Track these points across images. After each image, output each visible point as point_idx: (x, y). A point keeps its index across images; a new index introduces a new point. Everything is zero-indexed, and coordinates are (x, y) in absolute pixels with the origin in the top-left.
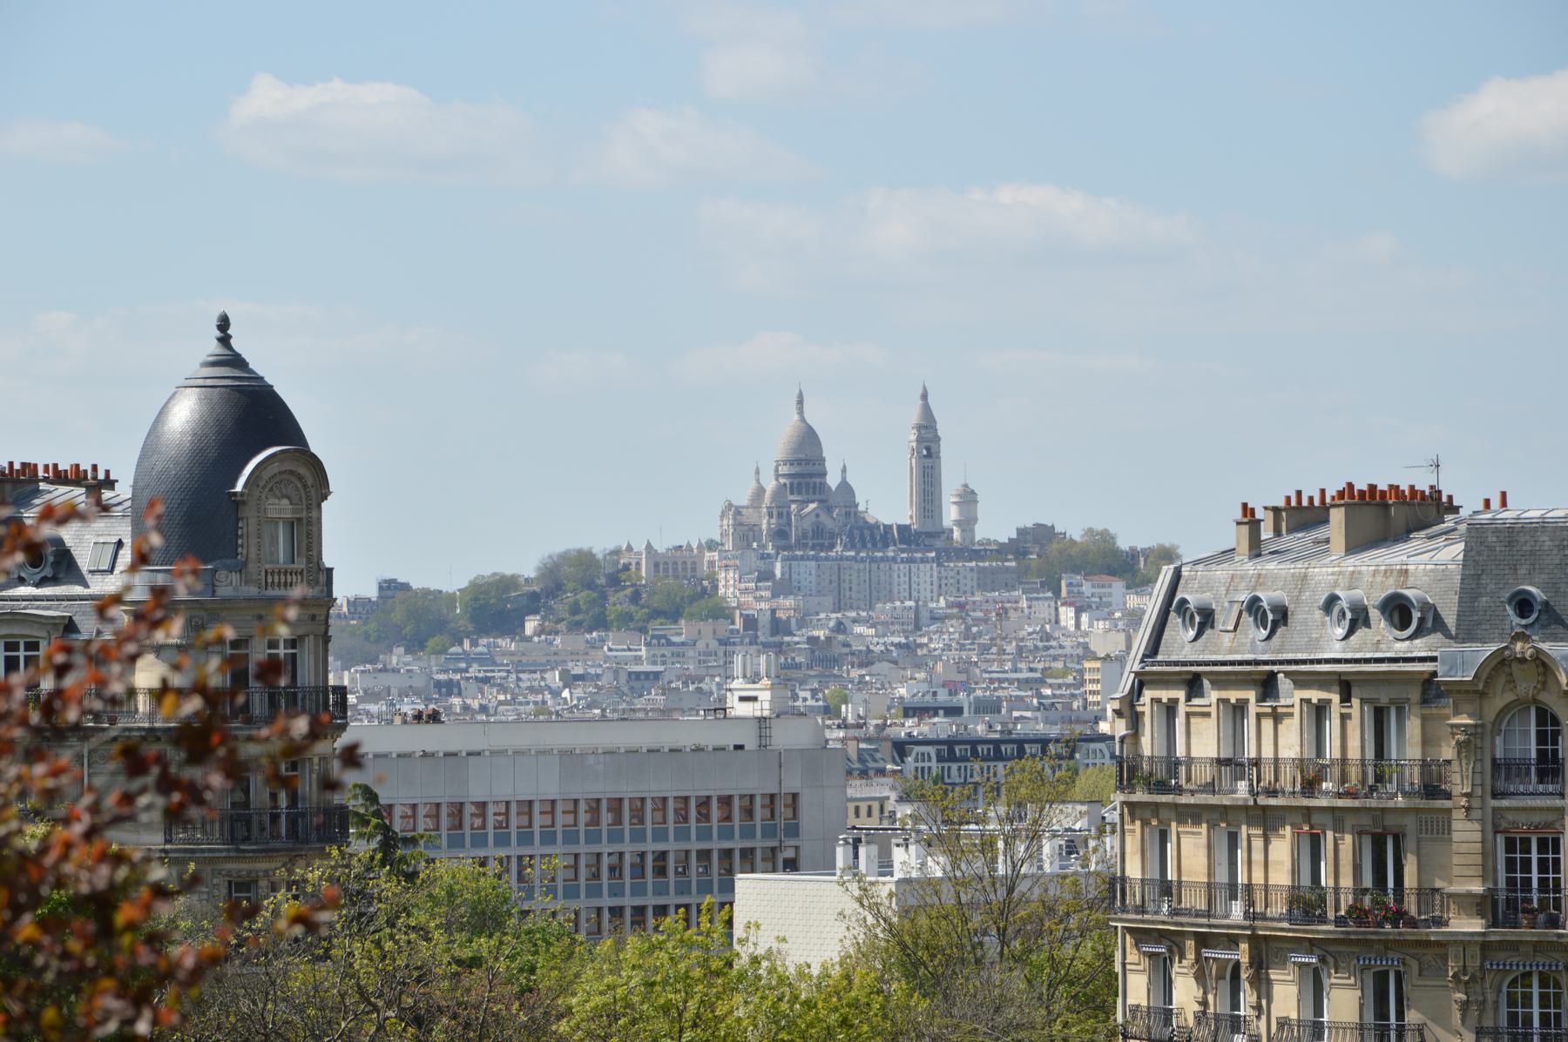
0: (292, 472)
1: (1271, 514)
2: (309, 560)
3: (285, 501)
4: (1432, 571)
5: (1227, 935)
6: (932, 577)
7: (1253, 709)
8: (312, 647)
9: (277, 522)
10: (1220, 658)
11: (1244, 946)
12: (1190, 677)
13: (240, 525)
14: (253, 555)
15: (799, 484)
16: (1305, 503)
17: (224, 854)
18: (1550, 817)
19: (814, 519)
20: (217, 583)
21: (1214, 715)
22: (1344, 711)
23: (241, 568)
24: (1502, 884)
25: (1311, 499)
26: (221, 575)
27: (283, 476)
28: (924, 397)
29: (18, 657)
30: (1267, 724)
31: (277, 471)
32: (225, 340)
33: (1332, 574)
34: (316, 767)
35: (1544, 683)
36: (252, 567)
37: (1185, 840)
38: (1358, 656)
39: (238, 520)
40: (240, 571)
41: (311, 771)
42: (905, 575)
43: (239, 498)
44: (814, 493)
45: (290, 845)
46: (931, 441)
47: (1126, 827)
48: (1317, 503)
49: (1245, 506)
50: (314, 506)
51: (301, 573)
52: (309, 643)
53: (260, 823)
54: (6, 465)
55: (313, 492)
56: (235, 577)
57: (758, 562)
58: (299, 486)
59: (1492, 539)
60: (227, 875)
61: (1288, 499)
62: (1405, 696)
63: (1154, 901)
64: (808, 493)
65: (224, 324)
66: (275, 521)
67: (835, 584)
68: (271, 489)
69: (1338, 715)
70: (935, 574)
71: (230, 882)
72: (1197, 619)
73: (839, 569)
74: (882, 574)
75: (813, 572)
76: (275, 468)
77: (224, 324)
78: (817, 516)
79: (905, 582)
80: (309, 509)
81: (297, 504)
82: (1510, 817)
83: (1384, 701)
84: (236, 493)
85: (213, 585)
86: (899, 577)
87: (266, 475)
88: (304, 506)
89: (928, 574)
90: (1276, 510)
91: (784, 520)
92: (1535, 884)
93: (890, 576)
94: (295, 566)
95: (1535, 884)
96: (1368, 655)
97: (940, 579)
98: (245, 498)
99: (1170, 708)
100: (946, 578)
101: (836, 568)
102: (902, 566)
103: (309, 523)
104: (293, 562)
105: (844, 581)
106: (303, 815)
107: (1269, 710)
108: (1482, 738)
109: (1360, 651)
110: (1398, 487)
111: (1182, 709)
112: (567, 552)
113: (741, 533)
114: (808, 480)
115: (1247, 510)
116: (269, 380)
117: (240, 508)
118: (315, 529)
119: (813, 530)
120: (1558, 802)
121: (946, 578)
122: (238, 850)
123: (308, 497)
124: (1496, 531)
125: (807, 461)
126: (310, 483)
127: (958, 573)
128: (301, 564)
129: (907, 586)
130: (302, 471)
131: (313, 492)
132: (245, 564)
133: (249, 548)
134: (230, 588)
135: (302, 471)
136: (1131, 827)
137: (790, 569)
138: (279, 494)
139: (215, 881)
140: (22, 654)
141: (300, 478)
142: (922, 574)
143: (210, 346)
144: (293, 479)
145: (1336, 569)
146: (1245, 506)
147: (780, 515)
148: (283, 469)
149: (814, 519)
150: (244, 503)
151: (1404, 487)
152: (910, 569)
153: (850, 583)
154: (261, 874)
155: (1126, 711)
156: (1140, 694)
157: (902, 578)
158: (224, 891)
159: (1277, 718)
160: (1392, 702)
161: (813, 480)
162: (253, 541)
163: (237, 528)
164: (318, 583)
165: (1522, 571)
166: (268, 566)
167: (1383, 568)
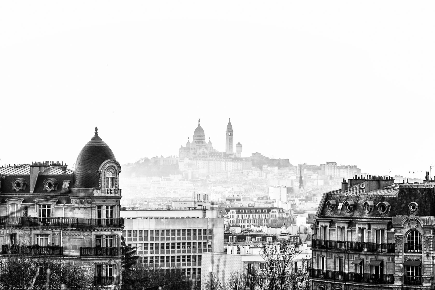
0: (112, 166)
1: (349, 181)
2: (116, 187)
3: (111, 173)
4: (390, 197)
5: (339, 284)
7: (346, 229)
8: (116, 208)
9: (108, 178)
10: (338, 216)
11: (343, 286)
12: (330, 221)
13: (100, 179)
14: (103, 186)
15: (199, 141)
16: (358, 178)
17: (95, 258)
18: (418, 258)
20: (94, 193)
21: (336, 230)
22: (369, 231)
23: (100, 189)
24: (406, 274)
25: (359, 177)
26: (95, 191)
27: (110, 167)
28: (230, 120)
29: (45, 209)
30: (350, 234)
31: (109, 166)
32: (96, 133)
33: (366, 197)
34: (117, 237)
35: (417, 225)
36: (103, 189)
37: (329, 260)
38: (372, 217)
39: (99, 177)
40: (100, 190)
41: (116, 238)
43: (100, 172)
45: (111, 257)
47: (314, 256)
48: (360, 178)
49: (344, 179)
50: (118, 174)
51: (114, 190)
52: (116, 207)
53: (103, 251)
54: (43, 163)
55: (117, 171)
56: (98, 191)
58: (114, 169)
59: (405, 190)
60: (95, 263)
61: (353, 177)
62: (384, 228)
63: (321, 275)
65: (96, 129)
66: (107, 178)
68: (107, 170)
69: (367, 232)
71: (96, 265)
72: (332, 207)
76: (108, 165)
77: (96, 129)
78: (203, 149)
80: (116, 175)
81: (113, 173)
82: (409, 257)
83: (379, 228)
84: (99, 171)
85: (93, 193)
87: (106, 167)
88: (115, 174)
90: (351, 180)
91: (195, 150)
92: (414, 274)
94: (113, 189)
95: (414, 274)
96: (375, 217)
97: (233, 165)
98: (101, 172)
99: (325, 228)
102: (224, 162)
103: (116, 178)
104: (112, 188)
106: (114, 249)
107: (350, 230)
108: (402, 238)
109: (372, 216)
110: (381, 176)
111: (328, 229)
115: (344, 181)
116: (107, 144)
117: (100, 174)
118: (117, 180)
120: (420, 255)
122: (98, 257)
123: (116, 172)
124: (406, 189)
125: (201, 136)
126: (117, 168)
127: (237, 164)
128: (114, 188)
129: (225, 167)
130: (115, 166)
131: (117, 170)
132: (101, 188)
133: (102, 184)
134: (97, 194)
135: (115, 166)
136: (315, 256)
138: (109, 171)
139: (93, 265)
140: (46, 208)
141: (114, 167)
143: (93, 135)
144: (113, 167)
145: (367, 196)
146: (344, 179)
147: (194, 149)
148: (110, 165)
150: (101, 173)
151: (383, 176)
154: (103, 263)
155: (314, 228)
156: (318, 224)
158: (94, 267)
159: (351, 231)
160: (380, 229)
162: (103, 182)
163: (99, 179)
164: (118, 193)
165: (413, 198)
166: (106, 189)
167: (378, 196)
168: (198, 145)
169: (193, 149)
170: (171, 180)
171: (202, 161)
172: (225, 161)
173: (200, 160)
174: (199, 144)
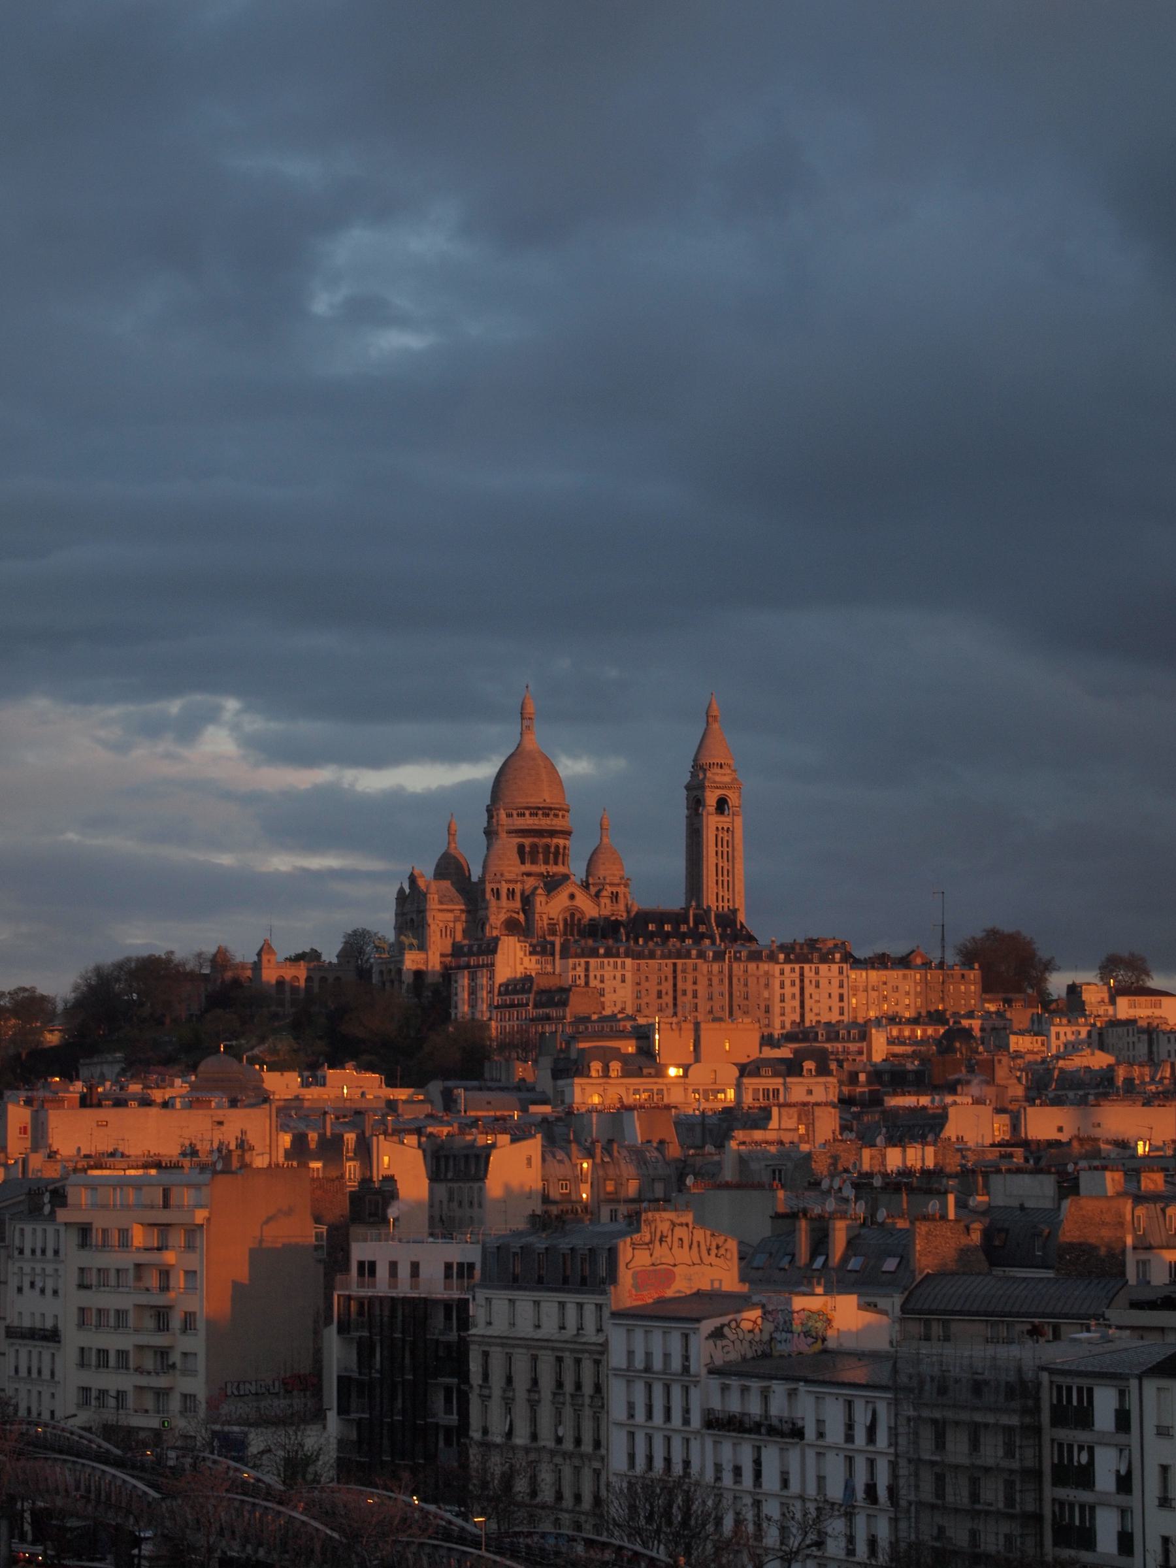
15: (534, 847)
19: (567, 903)
42: (793, 984)
44: (556, 863)
46: (730, 788)
57: (526, 959)
64: (546, 862)
67: (668, 999)
73: (675, 971)
74: (752, 981)
75: (629, 975)
79: (794, 996)
86: (782, 987)
89: (836, 983)
93: (767, 986)
101: (669, 971)
102: (787, 968)
105: (684, 993)
112: (129, 960)
113: (441, 924)
114: (548, 840)
119: (565, 920)
125: (547, 811)
129: (797, 1003)
137: (587, 970)
142: (823, 982)
149: (567, 903)
152: (802, 975)
153: (695, 996)
157: (788, 990)
161: (555, 841)
168: (528, 867)
169: (504, 892)
171: (628, 961)
172: (797, 961)
173: (608, 954)
174: (534, 862)
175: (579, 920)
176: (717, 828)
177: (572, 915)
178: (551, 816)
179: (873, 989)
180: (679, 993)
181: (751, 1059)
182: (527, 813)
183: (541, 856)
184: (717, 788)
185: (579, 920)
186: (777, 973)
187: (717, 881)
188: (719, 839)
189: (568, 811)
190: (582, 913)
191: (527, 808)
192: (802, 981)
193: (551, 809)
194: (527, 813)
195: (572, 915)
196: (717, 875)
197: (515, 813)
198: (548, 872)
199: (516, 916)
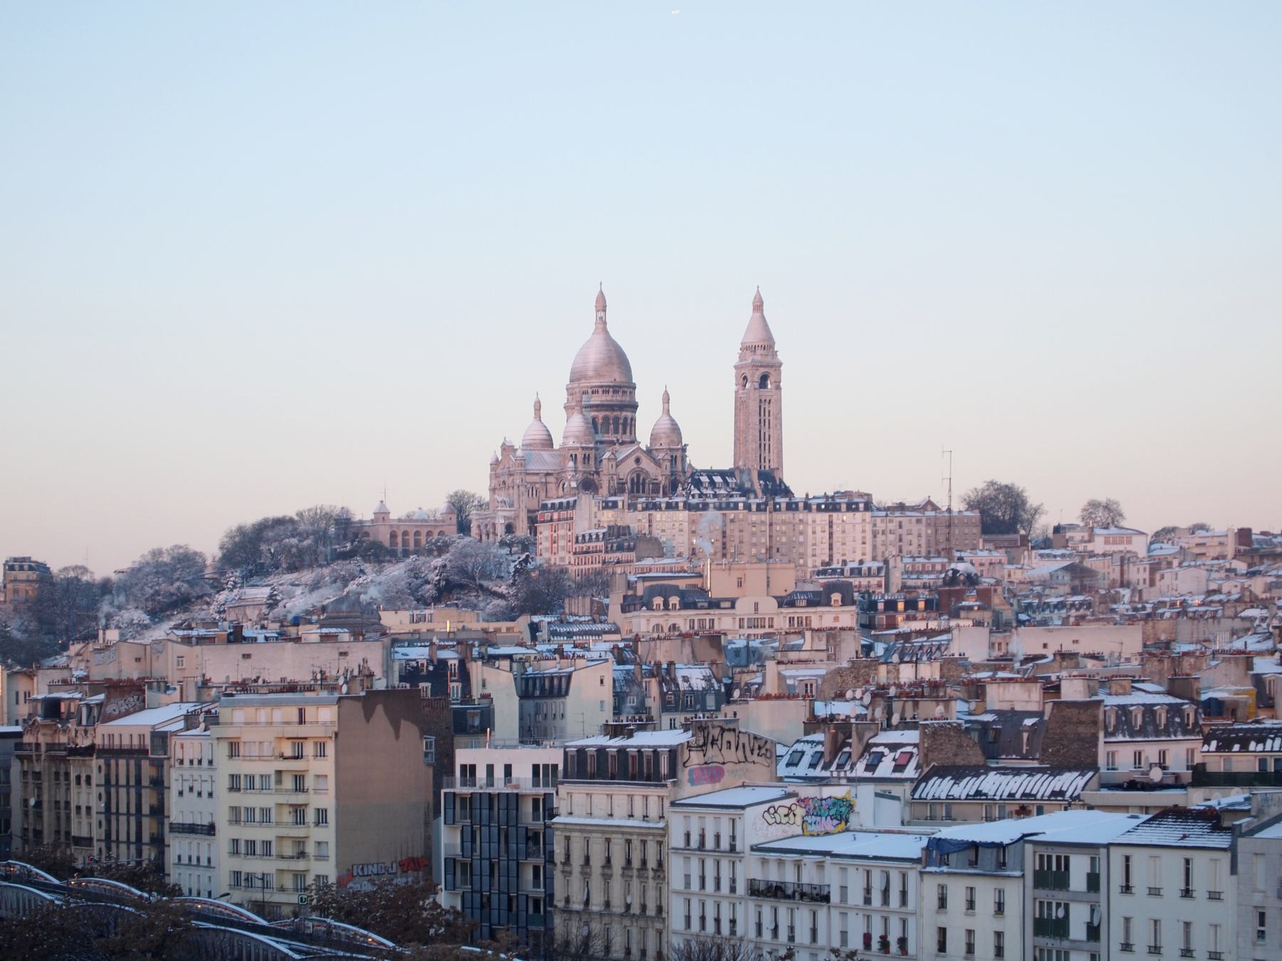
6: (864, 531)
15: (606, 419)
28: (758, 306)
57: (599, 514)
64: (616, 431)
70: (869, 528)
78: (638, 461)
86: (814, 533)
89: (859, 528)
97: (875, 535)
100: (883, 533)
114: (618, 413)
119: (632, 480)
121: (883, 533)
127: (900, 527)
147: (586, 459)
149: (635, 466)
157: (819, 534)
161: (624, 414)
170: (714, 604)
172: (826, 510)
175: (644, 480)
176: (761, 400)
177: (638, 476)
178: (620, 393)
179: (890, 533)
180: (727, 540)
181: (789, 592)
182: (600, 390)
183: (612, 427)
184: (761, 366)
185: (644, 480)
186: (810, 522)
187: (760, 445)
188: (762, 409)
189: (635, 388)
190: (647, 473)
191: (601, 387)
192: (831, 527)
193: (620, 387)
194: (600, 390)
195: (638, 476)
196: (760, 440)
197: (590, 391)
198: (618, 440)
199: (591, 477)
